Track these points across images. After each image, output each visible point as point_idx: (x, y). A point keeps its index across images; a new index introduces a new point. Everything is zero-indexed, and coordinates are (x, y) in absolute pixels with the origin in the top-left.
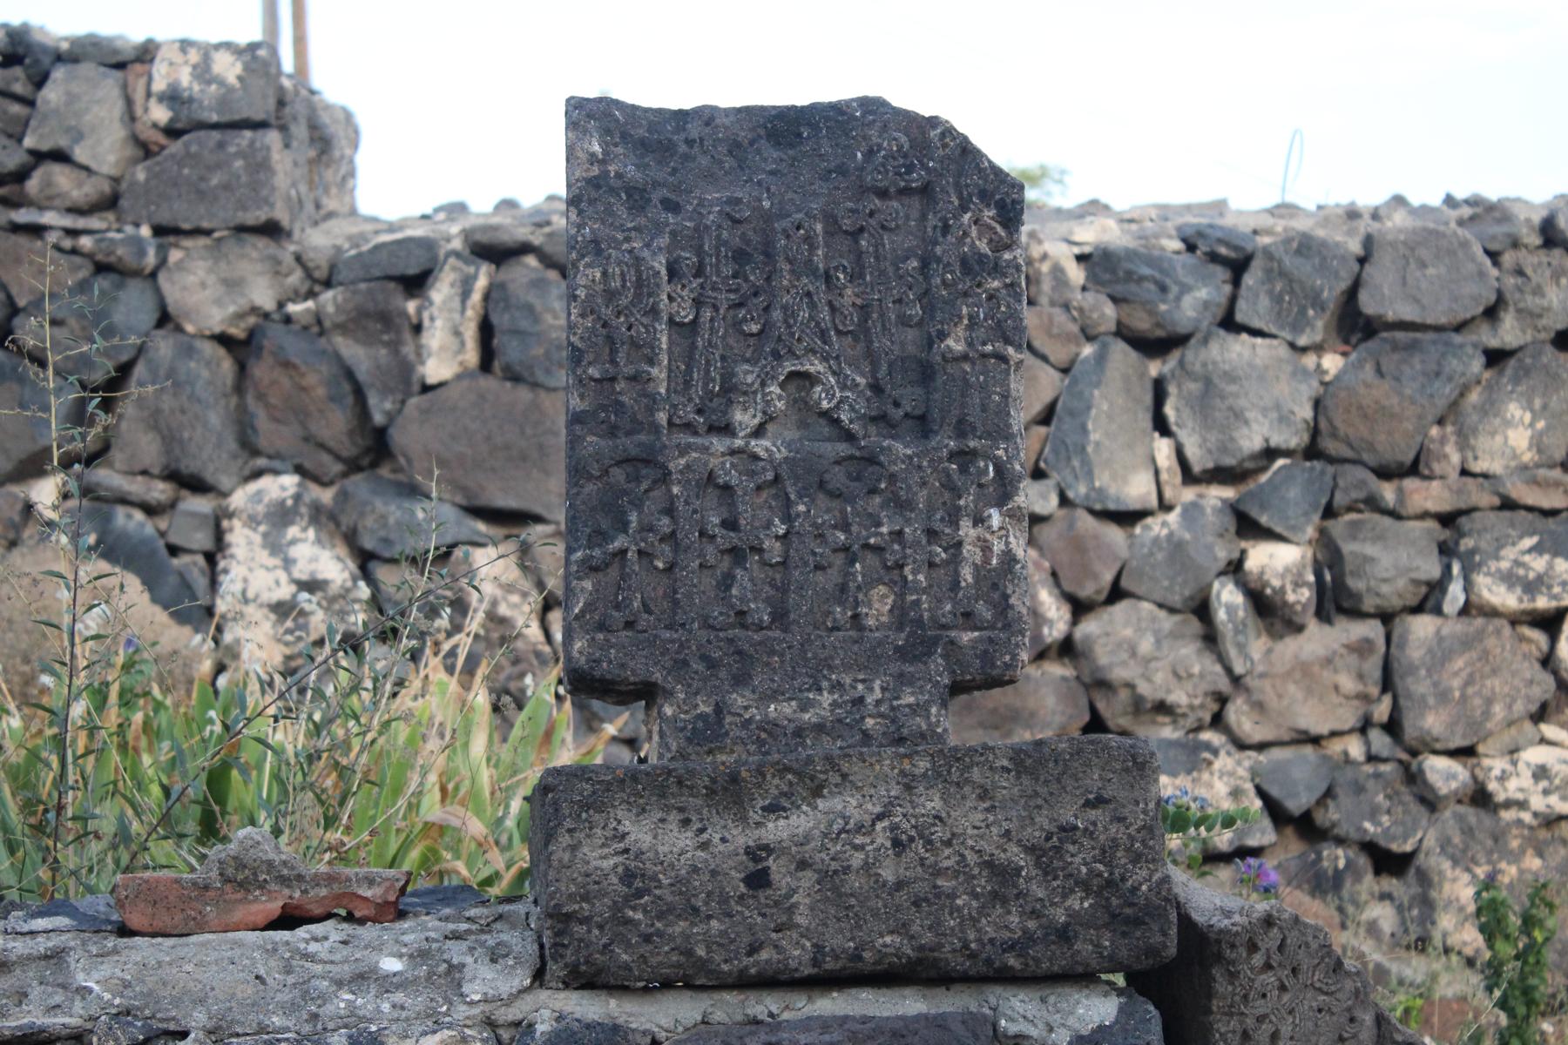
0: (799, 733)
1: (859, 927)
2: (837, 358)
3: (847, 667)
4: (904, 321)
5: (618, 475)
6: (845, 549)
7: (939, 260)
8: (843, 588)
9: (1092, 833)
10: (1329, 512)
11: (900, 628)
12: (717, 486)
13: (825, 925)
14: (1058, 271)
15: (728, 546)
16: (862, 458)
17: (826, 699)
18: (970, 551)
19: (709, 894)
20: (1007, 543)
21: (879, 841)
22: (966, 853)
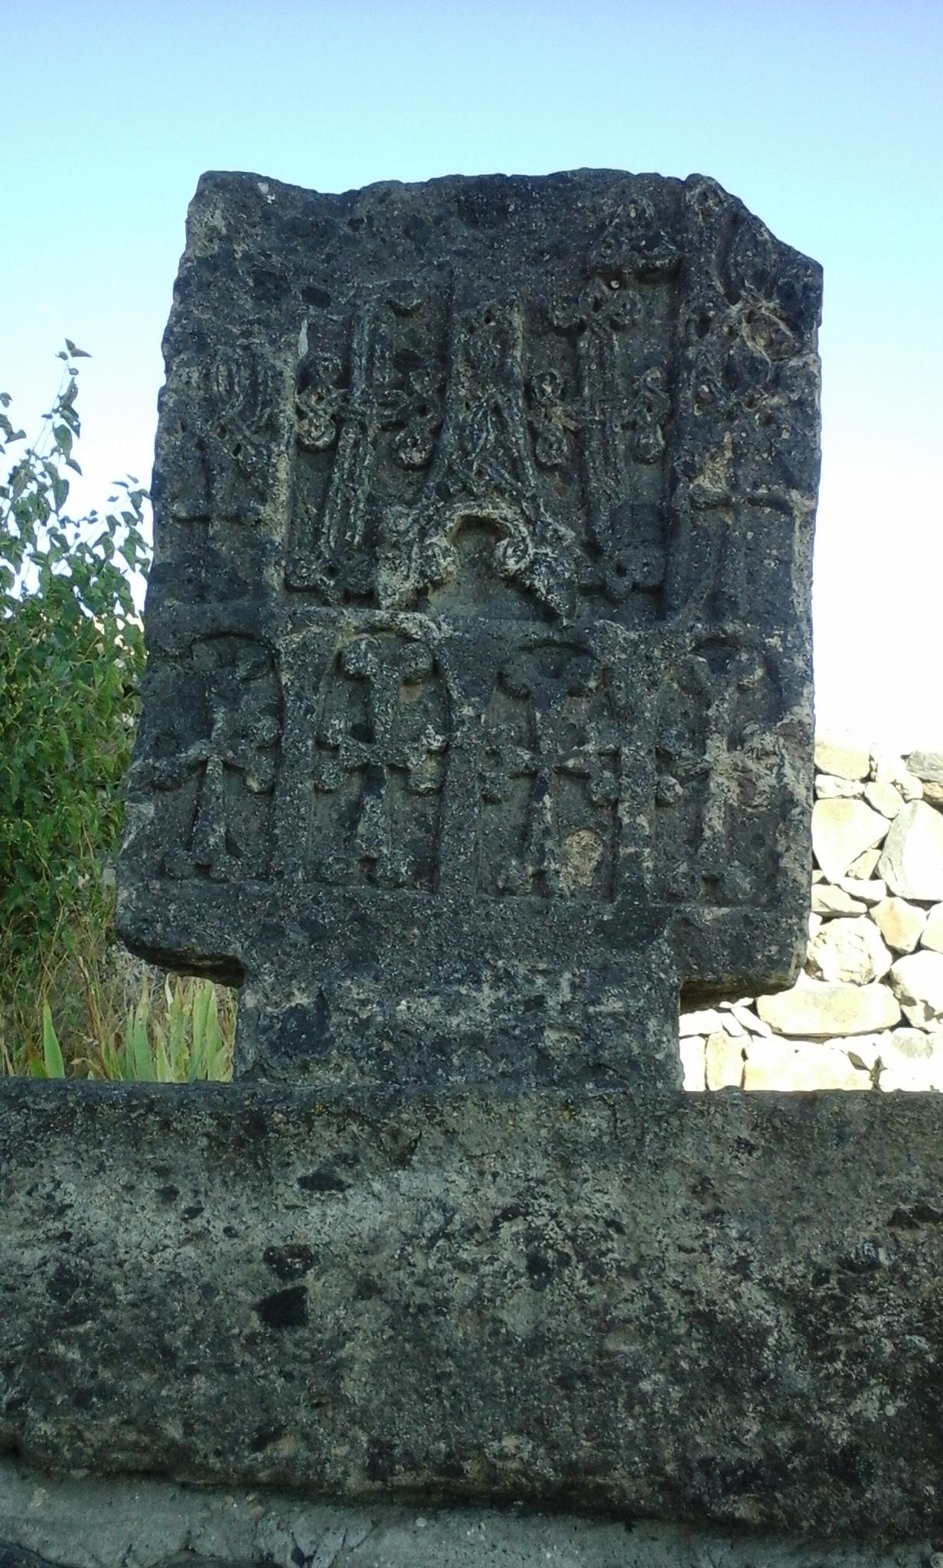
0: (441, 1046)
2: (534, 498)
3: (520, 951)
4: (638, 455)
5: (205, 657)
6: (532, 775)
7: (690, 366)
8: (525, 833)
9: (905, 1278)
11: (610, 896)
12: (349, 677)
13: (397, 1404)
15: (354, 762)
17: (487, 996)
18: (723, 785)
19: (197, 1327)
20: (780, 776)
21: (506, 1256)
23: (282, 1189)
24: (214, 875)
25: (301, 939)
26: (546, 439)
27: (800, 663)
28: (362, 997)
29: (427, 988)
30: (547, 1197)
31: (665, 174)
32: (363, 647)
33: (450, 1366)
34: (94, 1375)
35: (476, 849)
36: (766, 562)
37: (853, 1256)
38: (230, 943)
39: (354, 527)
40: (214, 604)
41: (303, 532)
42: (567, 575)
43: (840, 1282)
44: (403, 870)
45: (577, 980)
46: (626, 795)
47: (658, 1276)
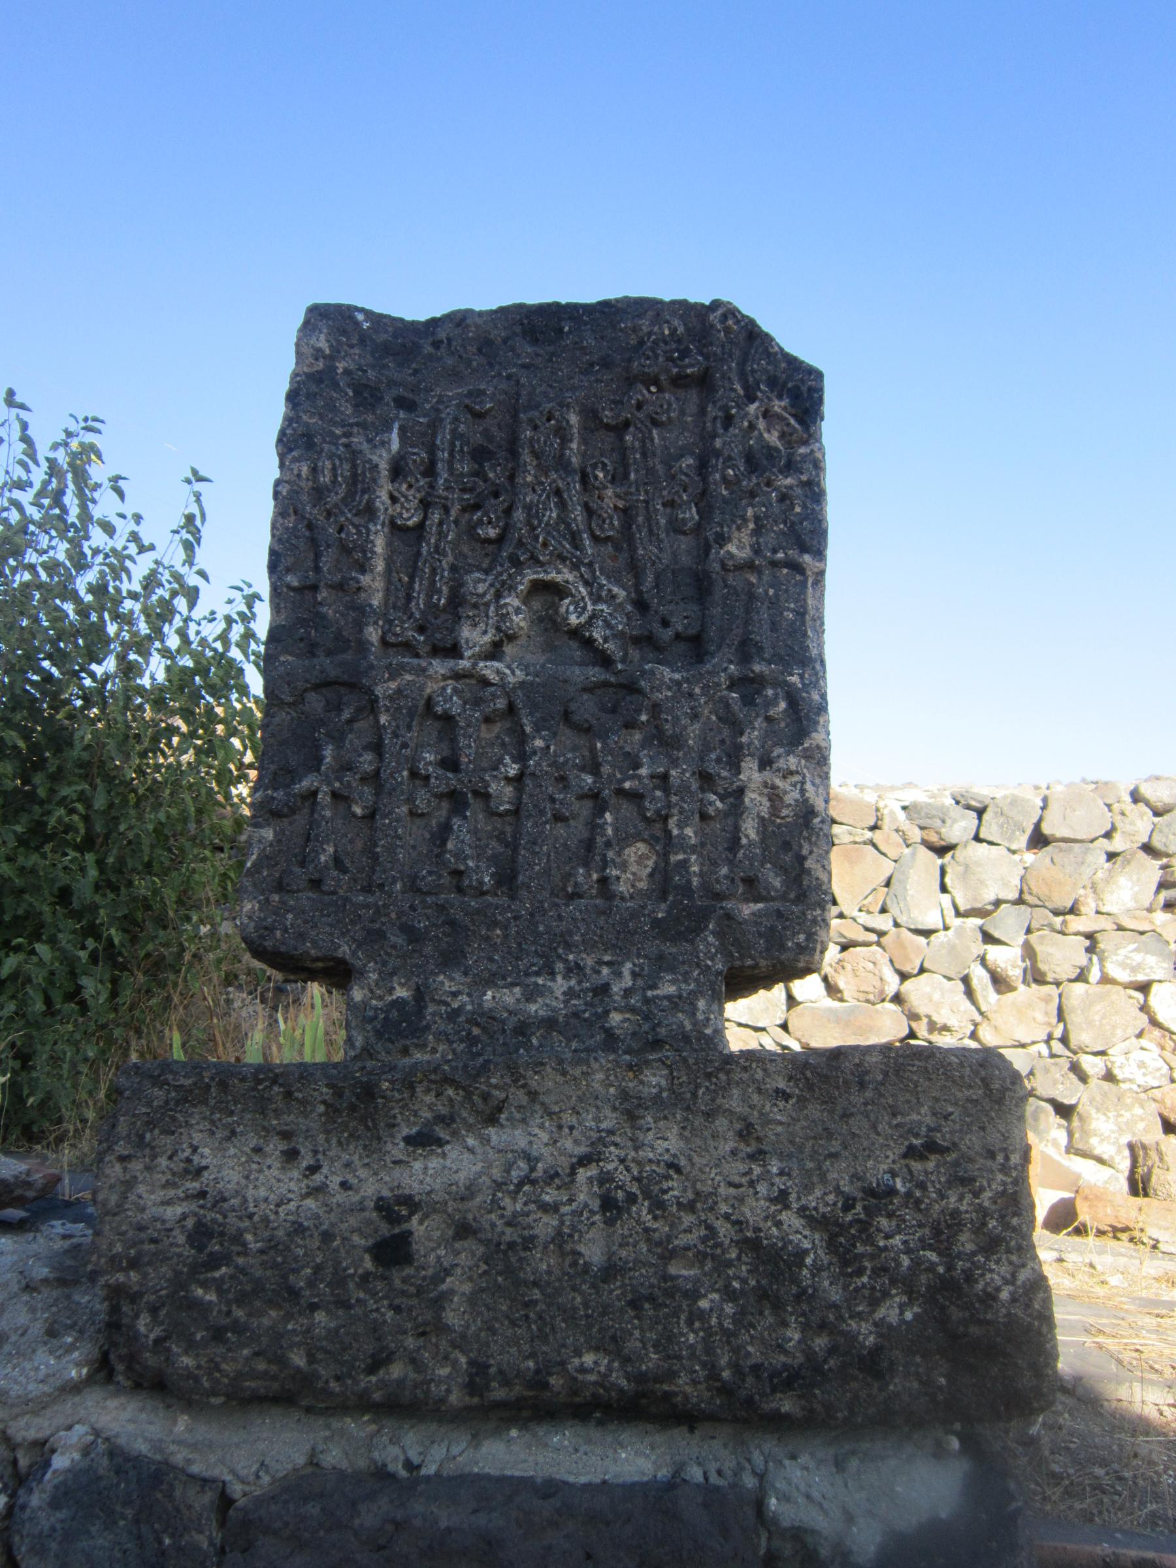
0: (523, 1029)
1: (544, 1338)
2: (590, 565)
3: (589, 945)
4: (676, 527)
5: (315, 703)
7: (717, 454)
8: (589, 845)
9: (918, 1202)
10: (1029, 931)
11: (663, 897)
12: (438, 718)
13: (492, 1330)
14: (892, 812)
15: (443, 788)
16: (621, 686)
17: (560, 985)
18: (756, 801)
19: (318, 1269)
20: (803, 791)
21: (582, 1197)
22: (718, 1224)
23: (389, 1147)
24: (325, 888)
25: (400, 941)
26: (600, 516)
27: (816, 697)
28: (453, 989)
29: (509, 980)
30: (616, 1145)
31: (692, 300)
32: (449, 691)
33: (536, 1294)
34: (229, 1313)
35: (548, 860)
36: (785, 613)
37: (874, 1185)
38: (340, 946)
39: (439, 592)
40: (322, 658)
41: (397, 597)
42: (620, 627)
43: (865, 1208)
44: (487, 879)
45: (637, 969)
46: (675, 811)
47: (711, 1209)
